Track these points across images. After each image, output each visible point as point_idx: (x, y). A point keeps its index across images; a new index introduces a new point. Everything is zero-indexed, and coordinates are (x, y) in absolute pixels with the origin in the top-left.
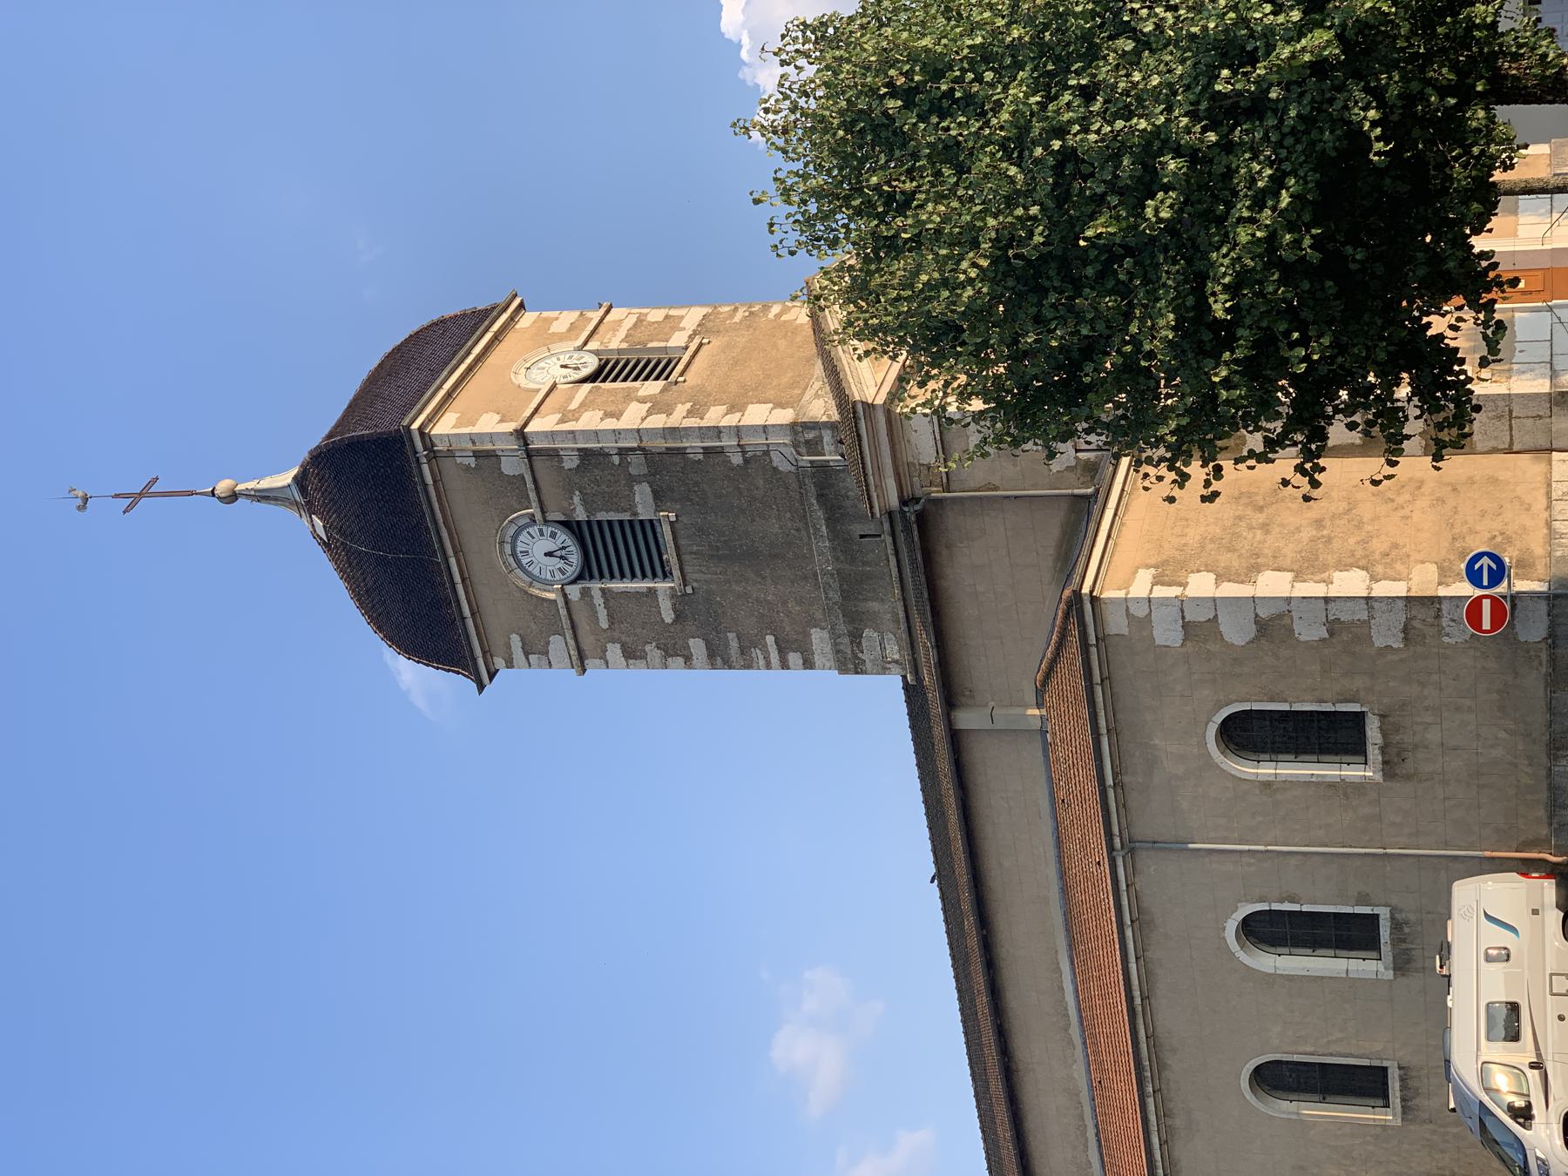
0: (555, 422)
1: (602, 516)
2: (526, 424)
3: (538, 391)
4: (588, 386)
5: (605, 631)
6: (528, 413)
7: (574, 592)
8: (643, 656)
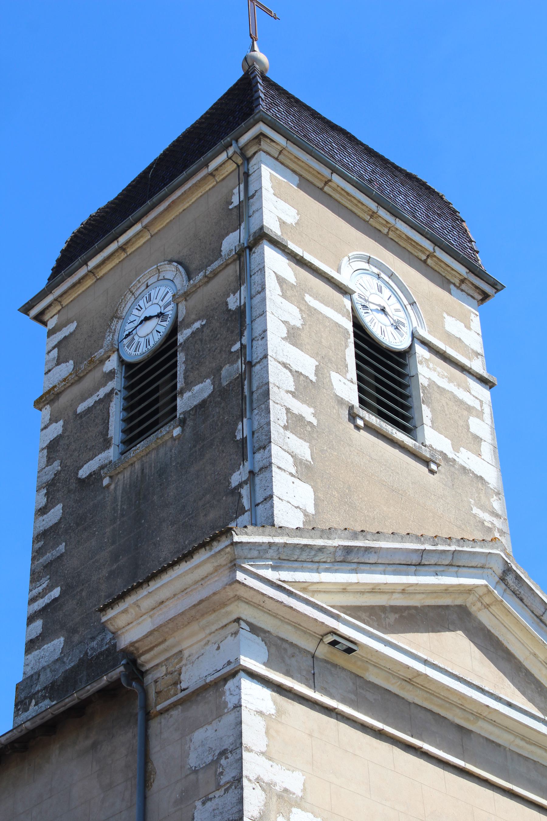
0: (279, 273)
1: (181, 357)
2: (276, 244)
3: (339, 271)
4: (349, 326)
5: (75, 411)
6: (292, 246)
7: (112, 364)
8: (50, 460)
